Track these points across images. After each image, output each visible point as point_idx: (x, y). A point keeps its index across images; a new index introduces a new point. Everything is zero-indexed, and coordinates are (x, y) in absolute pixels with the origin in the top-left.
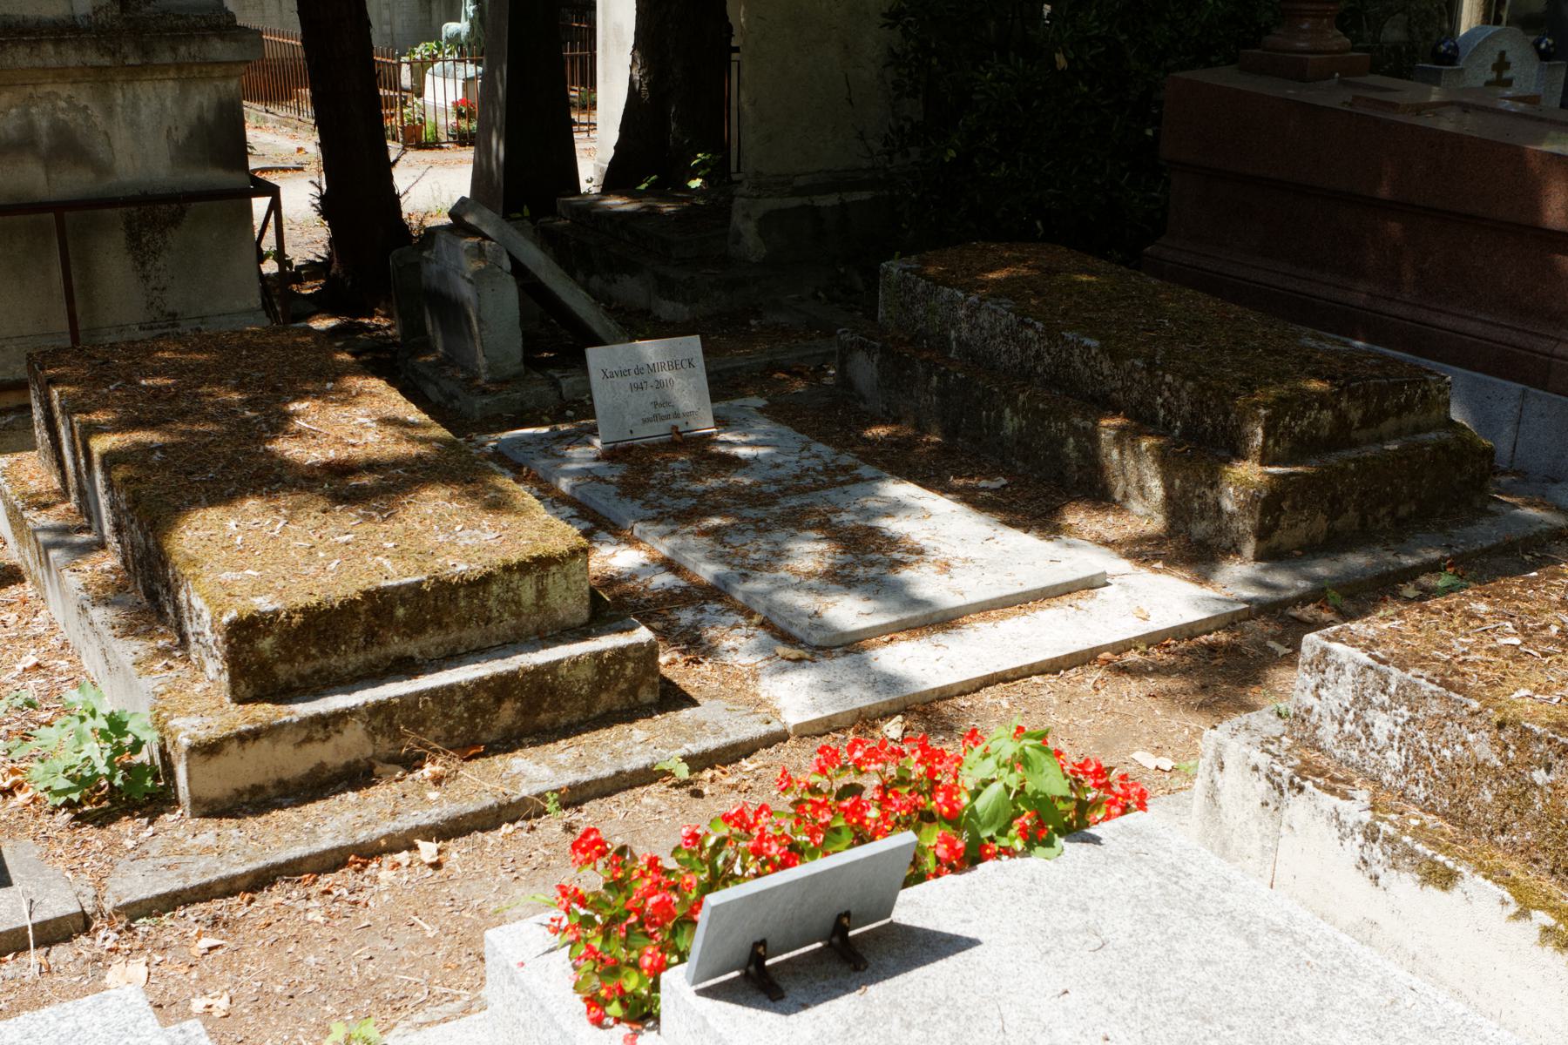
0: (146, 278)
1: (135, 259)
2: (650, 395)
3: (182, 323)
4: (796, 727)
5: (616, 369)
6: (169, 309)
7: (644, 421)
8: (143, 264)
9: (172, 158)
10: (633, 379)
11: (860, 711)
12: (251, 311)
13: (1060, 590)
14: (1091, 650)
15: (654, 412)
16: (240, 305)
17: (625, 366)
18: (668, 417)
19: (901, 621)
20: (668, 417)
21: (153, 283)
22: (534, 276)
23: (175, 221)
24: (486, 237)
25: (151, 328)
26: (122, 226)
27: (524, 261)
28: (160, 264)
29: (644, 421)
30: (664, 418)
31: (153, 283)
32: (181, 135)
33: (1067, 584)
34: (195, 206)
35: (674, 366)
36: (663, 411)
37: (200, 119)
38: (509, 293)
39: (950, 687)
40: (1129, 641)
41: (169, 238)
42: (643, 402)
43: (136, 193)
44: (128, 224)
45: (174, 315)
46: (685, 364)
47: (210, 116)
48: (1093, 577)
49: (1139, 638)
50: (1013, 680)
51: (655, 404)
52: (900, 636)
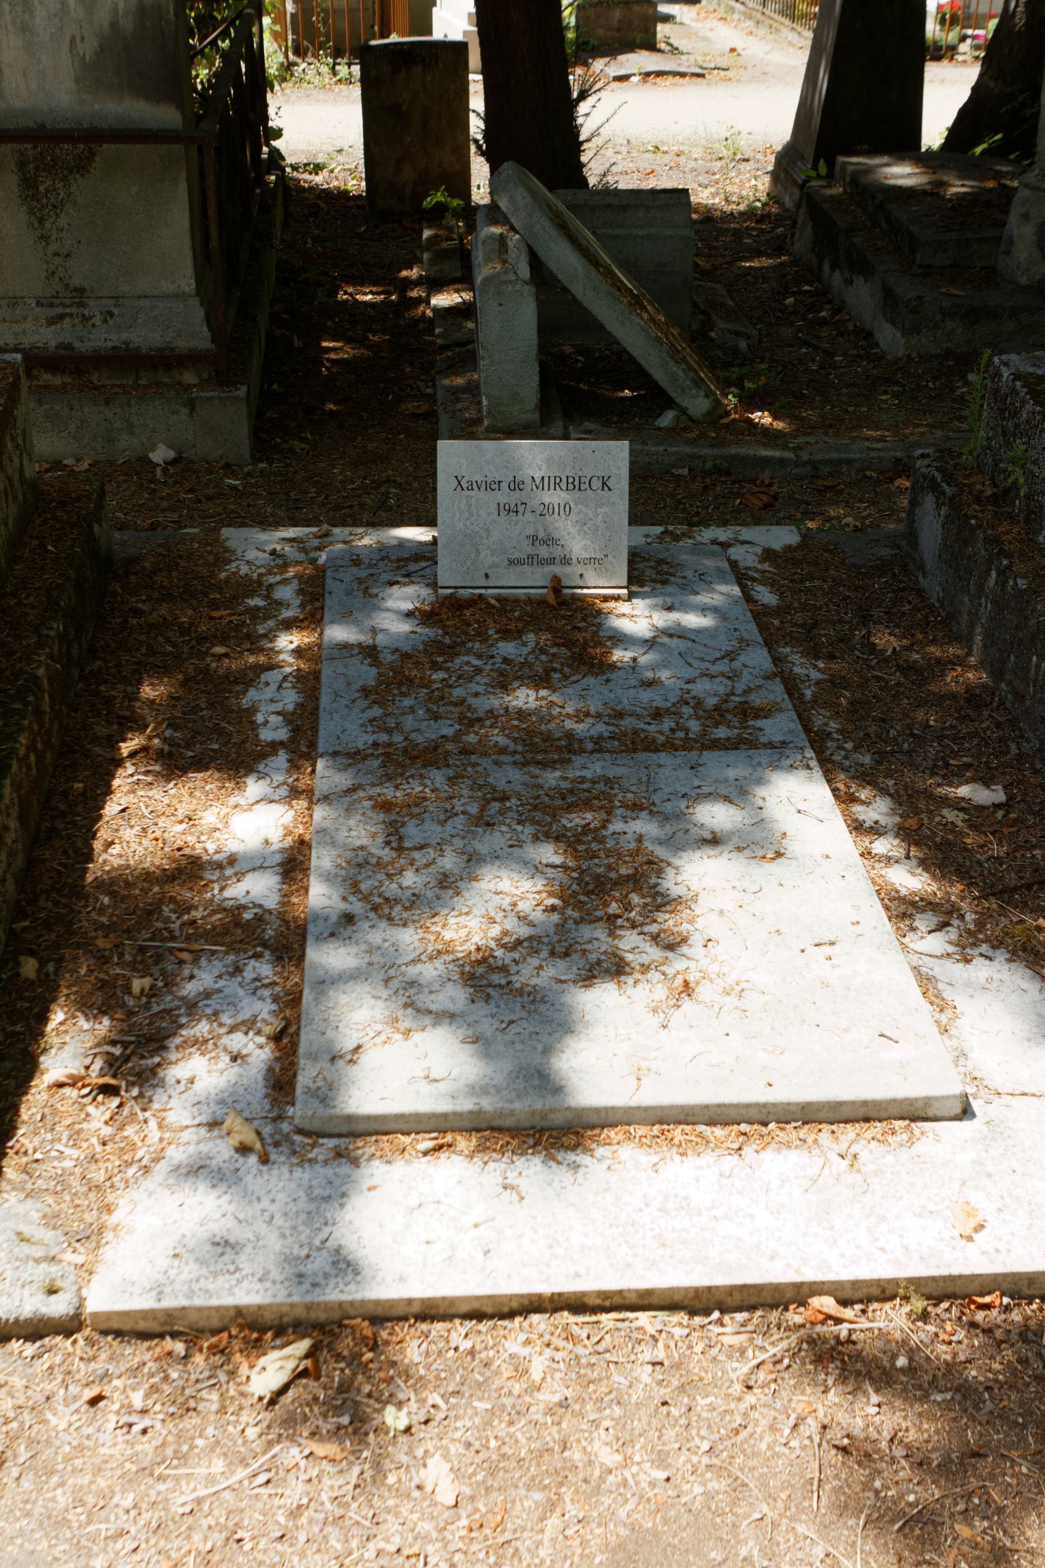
0: (45, 238)
1: (31, 213)
2: (527, 525)
3: (92, 303)
4: (95, 1315)
5: (479, 478)
6: (75, 282)
7: (511, 562)
8: (41, 220)
9: (77, 80)
10: (503, 496)
11: (239, 1311)
12: (180, 296)
13: (846, 1113)
14: (798, 1286)
15: (530, 550)
16: (166, 286)
17: (494, 475)
18: (551, 561)
19: (479, 1113)
20: (551, 561)
21: (53, 247)
22: (566, 290)
23: (81, 166)
24: (513, 228)
25: (51, 305)
26: (13, 167)
27: (553, 266)
28: (63, 222)
29: (511, 562)
30: (543, 562)
31: (53, 247)
32: (88, 47)
33: (865, 1103)
34: (107, 149)
35: (575, 484)
36: (544, 552)
37: (114, 26)
38: (525, 314)
39: (452, 1301)
40: (896, 1282)
41: (74, 188)
42: (512, 534)
43: (31, 124)
44: (22, 165)
45: (81, 291)
46: (596, 484)
47: (127, 24)
48: (928, 1101)
49: (917, 1283)
50: (595, 1310)
51: (534, 539)
52: (463, 1143)
